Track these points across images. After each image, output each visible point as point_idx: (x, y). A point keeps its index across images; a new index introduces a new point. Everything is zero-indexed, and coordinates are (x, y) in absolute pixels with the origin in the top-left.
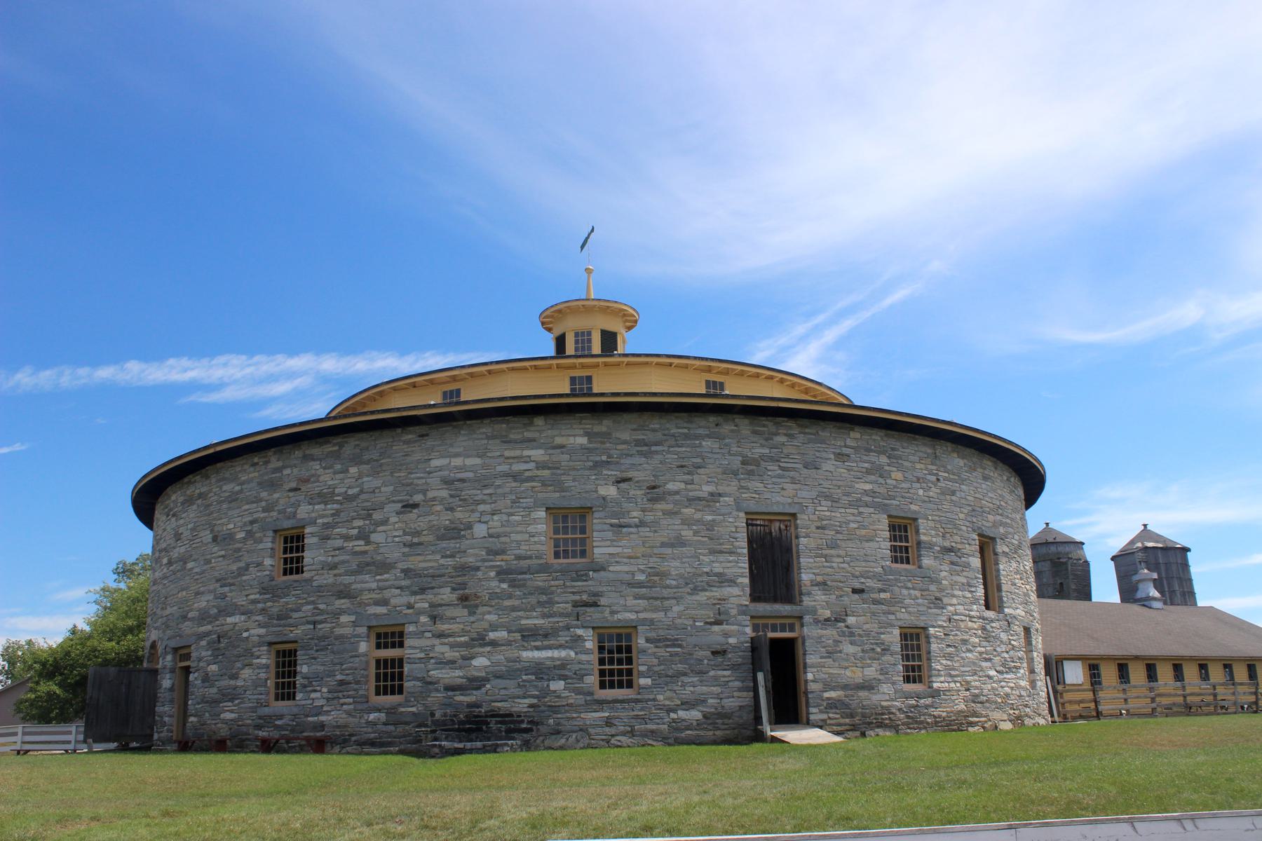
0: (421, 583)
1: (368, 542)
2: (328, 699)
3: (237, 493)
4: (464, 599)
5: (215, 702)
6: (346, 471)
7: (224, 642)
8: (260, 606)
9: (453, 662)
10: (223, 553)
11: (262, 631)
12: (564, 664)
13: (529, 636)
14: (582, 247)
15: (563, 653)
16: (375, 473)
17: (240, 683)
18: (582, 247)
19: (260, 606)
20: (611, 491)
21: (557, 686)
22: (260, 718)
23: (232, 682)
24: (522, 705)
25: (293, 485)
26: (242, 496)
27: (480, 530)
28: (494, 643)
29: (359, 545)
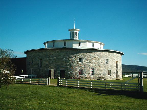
0: (95, 65)
1: (91, 60)
4: (99, 67)
9: (98, 72)
12: (106, 73)
13: (104, 70)
15: (106, 72)
20: (109, 58)
21: (106, 75)
24: (104, 76)
27: (101, 60)
28: (102, 71)
29: (90, 61)
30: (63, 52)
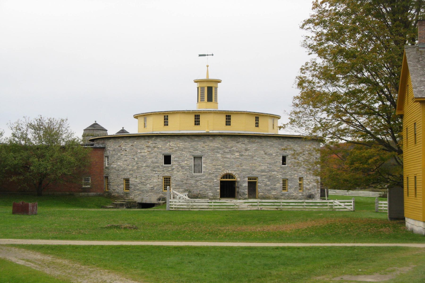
2: (294, 191)
3: (272, 145)
5: (269, 190)
6: (295, 145)
7: (271, 178)
8: (280, 171)
10: (269, 157)
11: (281, 176)
14: (200, 55)
16: (299, 147)
17: (277, 186)
18: (200, 55)
19: (280, 171)
22: (282, 194)
23: (275, 186)
25: (286, 146)
26: (274, 146)
30: (254, 142)
